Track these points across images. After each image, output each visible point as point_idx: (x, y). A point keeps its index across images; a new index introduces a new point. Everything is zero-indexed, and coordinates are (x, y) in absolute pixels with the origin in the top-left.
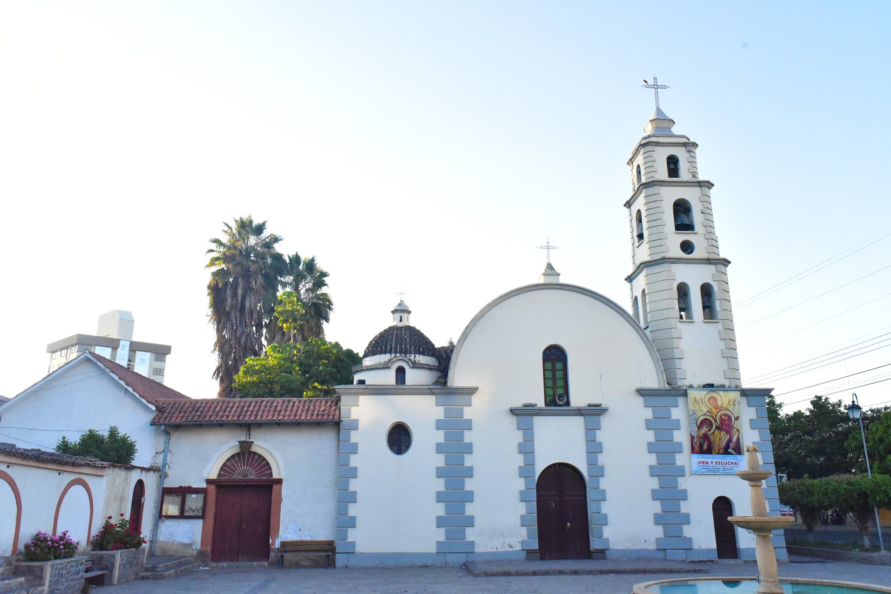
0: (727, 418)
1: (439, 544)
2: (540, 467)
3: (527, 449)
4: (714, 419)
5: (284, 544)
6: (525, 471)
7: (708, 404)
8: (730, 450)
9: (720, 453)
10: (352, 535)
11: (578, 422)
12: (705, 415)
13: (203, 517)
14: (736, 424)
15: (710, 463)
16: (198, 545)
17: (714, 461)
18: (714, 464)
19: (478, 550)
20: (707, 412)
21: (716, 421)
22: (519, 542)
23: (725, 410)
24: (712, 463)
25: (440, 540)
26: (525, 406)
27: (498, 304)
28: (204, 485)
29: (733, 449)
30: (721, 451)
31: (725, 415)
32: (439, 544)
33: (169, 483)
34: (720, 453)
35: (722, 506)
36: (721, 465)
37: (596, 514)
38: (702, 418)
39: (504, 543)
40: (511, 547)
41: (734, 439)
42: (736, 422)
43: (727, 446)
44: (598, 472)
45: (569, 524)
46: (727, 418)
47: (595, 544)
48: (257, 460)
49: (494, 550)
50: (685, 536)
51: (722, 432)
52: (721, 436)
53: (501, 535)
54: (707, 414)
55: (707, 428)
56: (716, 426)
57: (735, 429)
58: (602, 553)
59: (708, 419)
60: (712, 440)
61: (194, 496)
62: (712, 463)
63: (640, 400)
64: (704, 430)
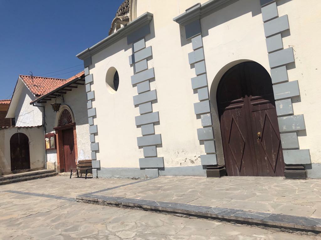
1: (140, 160)
5: (81, 162)
16: (56, 164)
22: (199, 157)
25: (141, 158)
26: (186, 11)
32: (140, 160)
37: (285, 118)
39: (186, 159)
40: (192, 162)
45: (259, 133)
47: (289, 158)
48: (67, 114)
49: (179, 166)
53: (183, 151)
61: (52, 138)
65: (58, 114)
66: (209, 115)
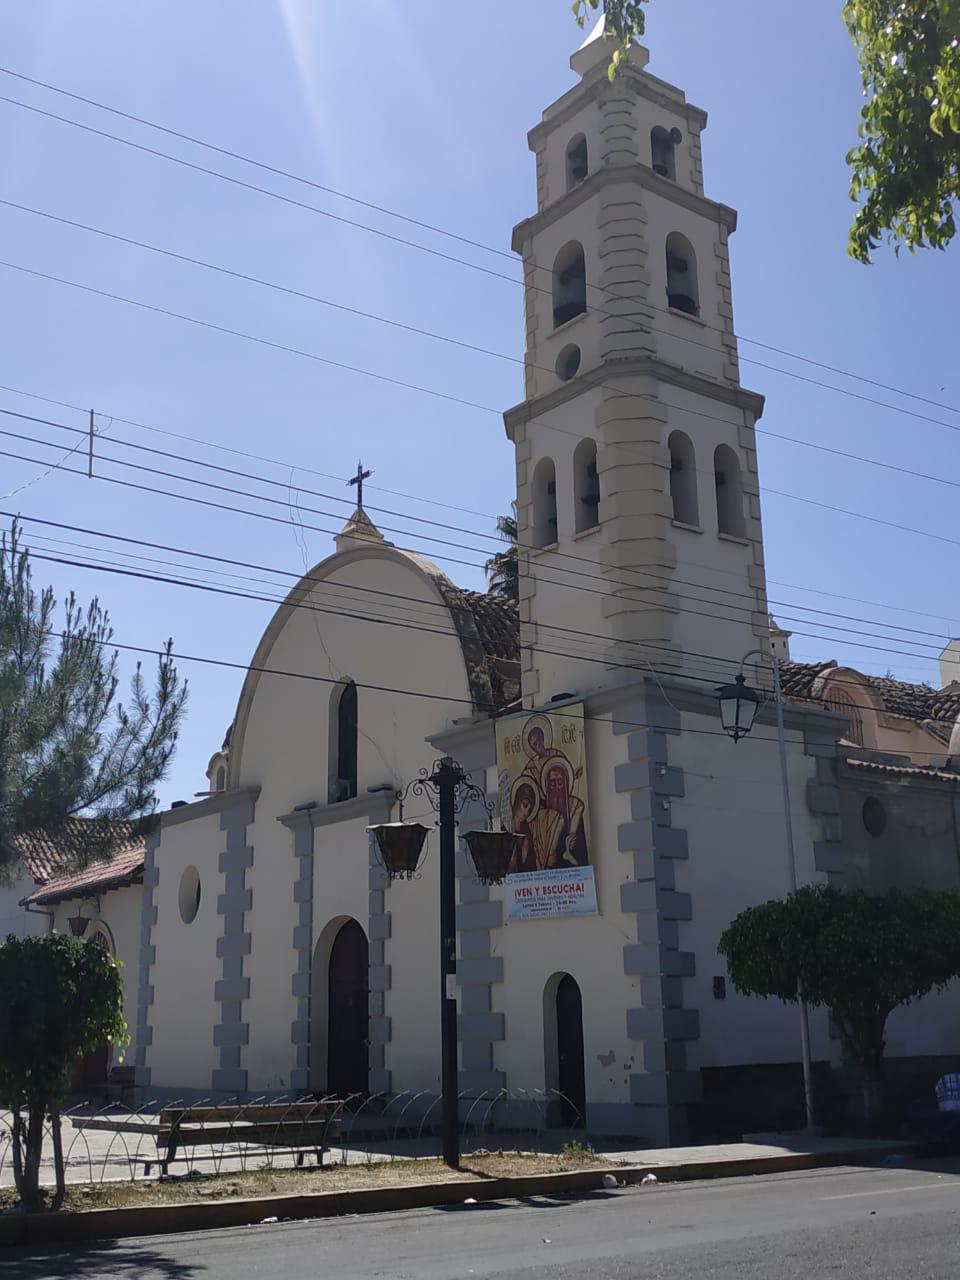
0: (559, 776)
3: (304, 891)
4: (537, 783)
7: (529, 750)
8: (567, 856)
9: (550, 865)
10: (153, 1057)
12: (522, 776)
14: (579, 788)
15: (534, 891)
17: (541, 884)
18: (541, 891)
20: (526, 769)
21: (540, 786)
23: (557, 756)
24: (537, 890)
27: (286, 620)
29: (572, 852)
30: (551, 860)
31: (556, 768)
34: (550, 865)
35: (565, 994)
36: (552, 894)
38: (519, 783)
41: (574, 828)
42: (577, 780)
43: (561, 848)
46: (559, 776)
47: (375, 1086)
50: (497, 1071)
51: (551, 811)
52: (551, 819)
54: (525, 773)
55: (526, 806)
56: (541, 799)
57: (576, 801)
59: (530, 787)
60: (534, 836)
62: (537, 890)
64: (523, 811)
66: (307, 999)
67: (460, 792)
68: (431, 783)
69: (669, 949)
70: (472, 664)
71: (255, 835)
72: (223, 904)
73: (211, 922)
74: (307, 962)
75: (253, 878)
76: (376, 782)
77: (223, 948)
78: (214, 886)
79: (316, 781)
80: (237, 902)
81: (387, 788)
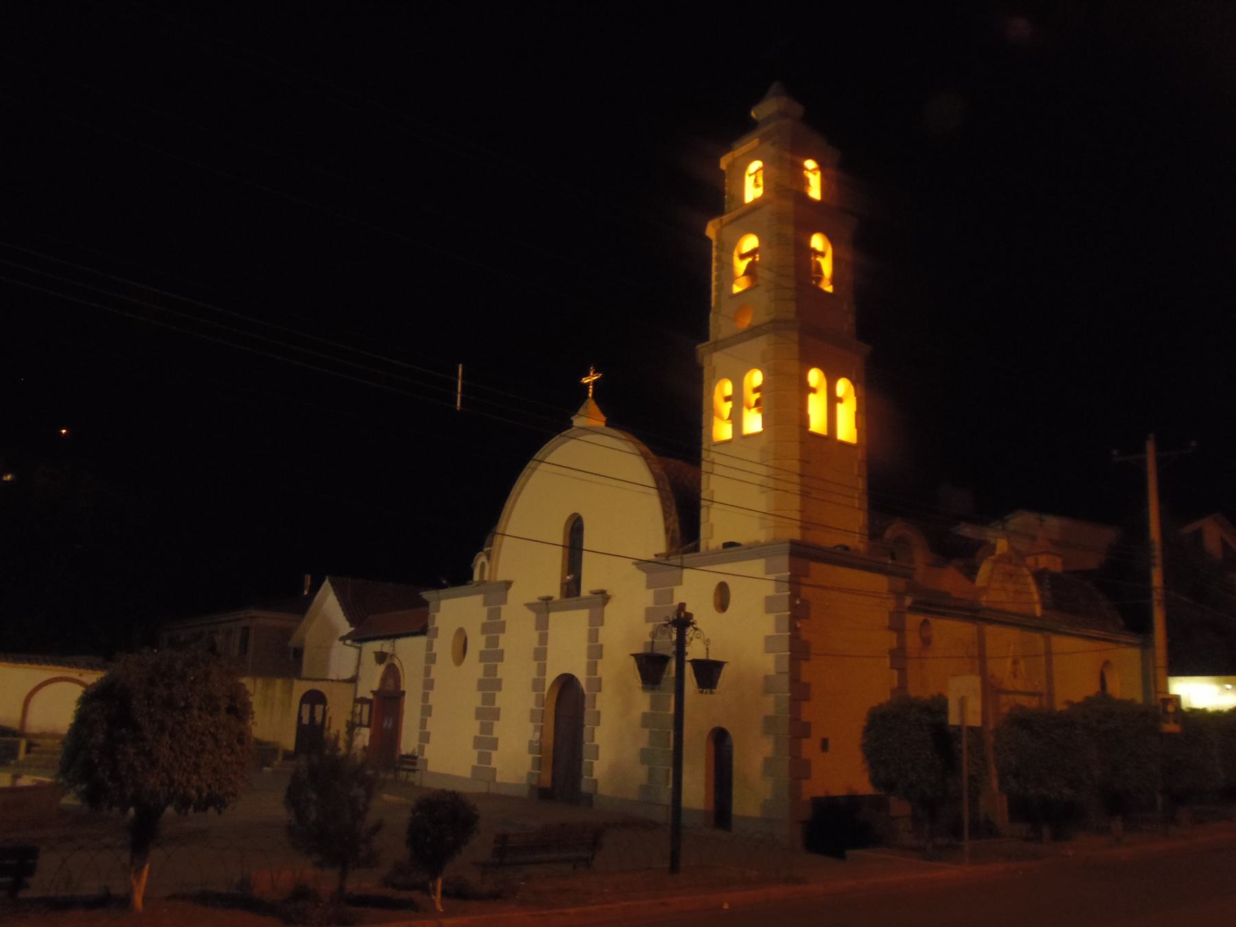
2: (550, 677)
3: (540, 655)
6: (537, 684)
11: (584, 615)
13: (368, 726)
19: (498, 779)
28: (370, 696)
33: (359, 696)
44: (597, 685)
47: (584, 787)
58: (589, 799)
63: (643, 576)
65: (382, 668)
67: (689, 632)
68: (670, 626)
69: (795, 718)
70: (667, 516)
71: (506, 612)
72: (484, 656)
73: (473, 667)
74: (540, 701)
75: (504, 641)
76: (596, 588)
77: (482, 685)
78: (477, 643)
79: (552, 587)
80: (493, 656)
81: (603, 592)
